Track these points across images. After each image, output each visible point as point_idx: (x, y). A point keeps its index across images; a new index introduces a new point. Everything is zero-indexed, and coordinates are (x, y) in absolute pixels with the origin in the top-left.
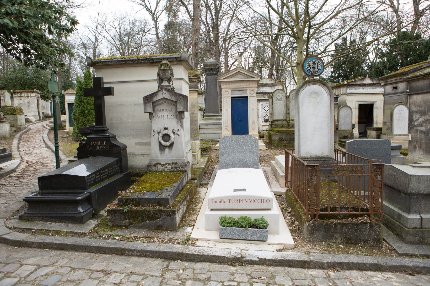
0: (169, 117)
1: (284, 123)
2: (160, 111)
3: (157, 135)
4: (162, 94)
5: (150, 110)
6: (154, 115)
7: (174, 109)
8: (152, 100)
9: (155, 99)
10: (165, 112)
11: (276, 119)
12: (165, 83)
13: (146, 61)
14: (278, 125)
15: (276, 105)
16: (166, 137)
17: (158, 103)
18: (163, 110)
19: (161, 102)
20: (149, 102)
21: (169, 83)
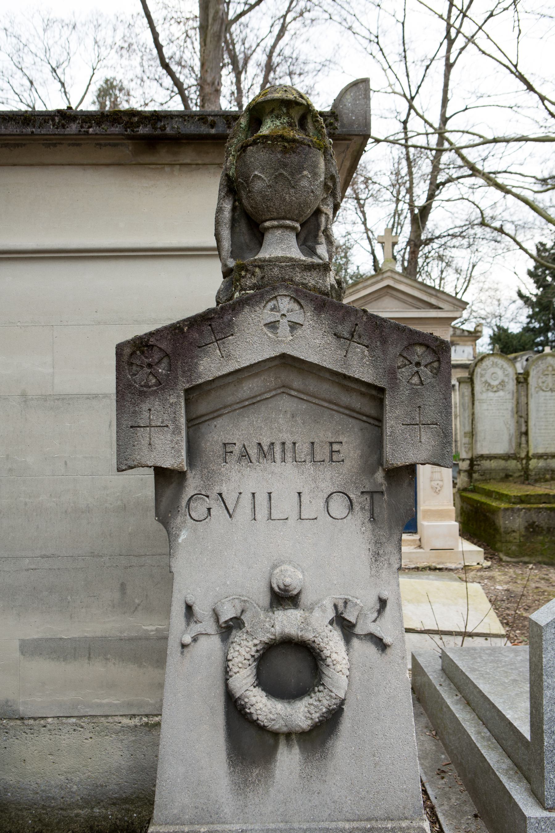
0: (313, 506)
1: (513, 464)
2: (245, 455)
3: (216, 641)
5: (170, 452)
6: (192, 485)
7: (351, 446)
8: (190, 370)
9: (211, 365)
10: (277, 467)
12: (281, 247)
13: (116, 129)
15: (485, 406)
16: (292, 664)
17: (230, 396)
19: (250, 387)
20: (163, 385)
21: (312, 252)
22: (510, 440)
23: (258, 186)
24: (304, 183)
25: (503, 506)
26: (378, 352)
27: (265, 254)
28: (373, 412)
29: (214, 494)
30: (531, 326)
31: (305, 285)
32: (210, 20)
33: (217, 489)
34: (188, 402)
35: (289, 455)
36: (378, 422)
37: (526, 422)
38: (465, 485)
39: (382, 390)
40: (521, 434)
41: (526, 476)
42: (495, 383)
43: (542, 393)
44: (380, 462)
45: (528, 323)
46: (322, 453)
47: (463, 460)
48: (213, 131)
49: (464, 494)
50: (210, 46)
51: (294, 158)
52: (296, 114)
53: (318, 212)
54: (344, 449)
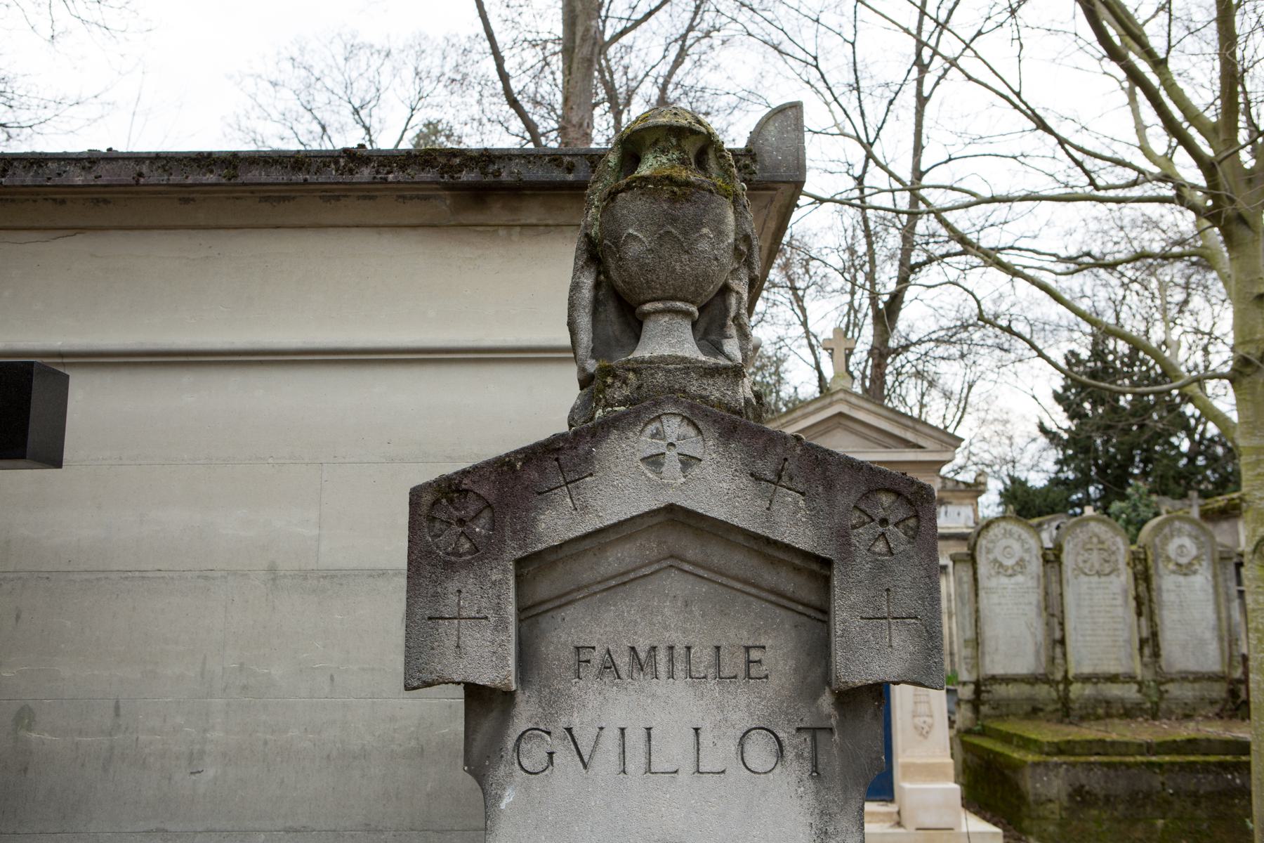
0: (719, 752)
1: (1043, 691)
2: (609, 666)
4: (654, 461)
5: (490, 659)
6: (525, 715)
7: (780, 653)
8: (526, 529)
9: (556, 523)
10: (661, 686)
11: (998, 670)
12: (669, 341)
13: (428, 175)
14: (1008, 702)
15: (995, 599)
17: (588, 570)
18: (642, 663)
19: (619, 558)
20: (482, 552)
21: (717, 349)
22: (1037, 653)
23: (633, 250)
24: (703, 245)
25: (1030, 758)
26: (821, 503)
27: (644, 351)
28: (813, 598)
29: (559, 730)
30: (1062, 475)
31: (705, 399)
32: (578, 41)
33: (563, 721)
34: (519, 578)
35: (680, 666)
36: (822, 613)
37: (1062, 624)
38: (968, 724)
39: (827, 563)
40: (1055, 642)
41: (1065, 711)
42: (1009, 562)
43: (1083, 578)
44: (826, 680)
45: (1057, 473)
46: (733, 663)
47: (964, 684)
48: (571, 177)
49: (968, 739)
50: (577, 74)
51: (689, 210)
52: (691, 147)
53: (725, 290)
54: (768, 657)
